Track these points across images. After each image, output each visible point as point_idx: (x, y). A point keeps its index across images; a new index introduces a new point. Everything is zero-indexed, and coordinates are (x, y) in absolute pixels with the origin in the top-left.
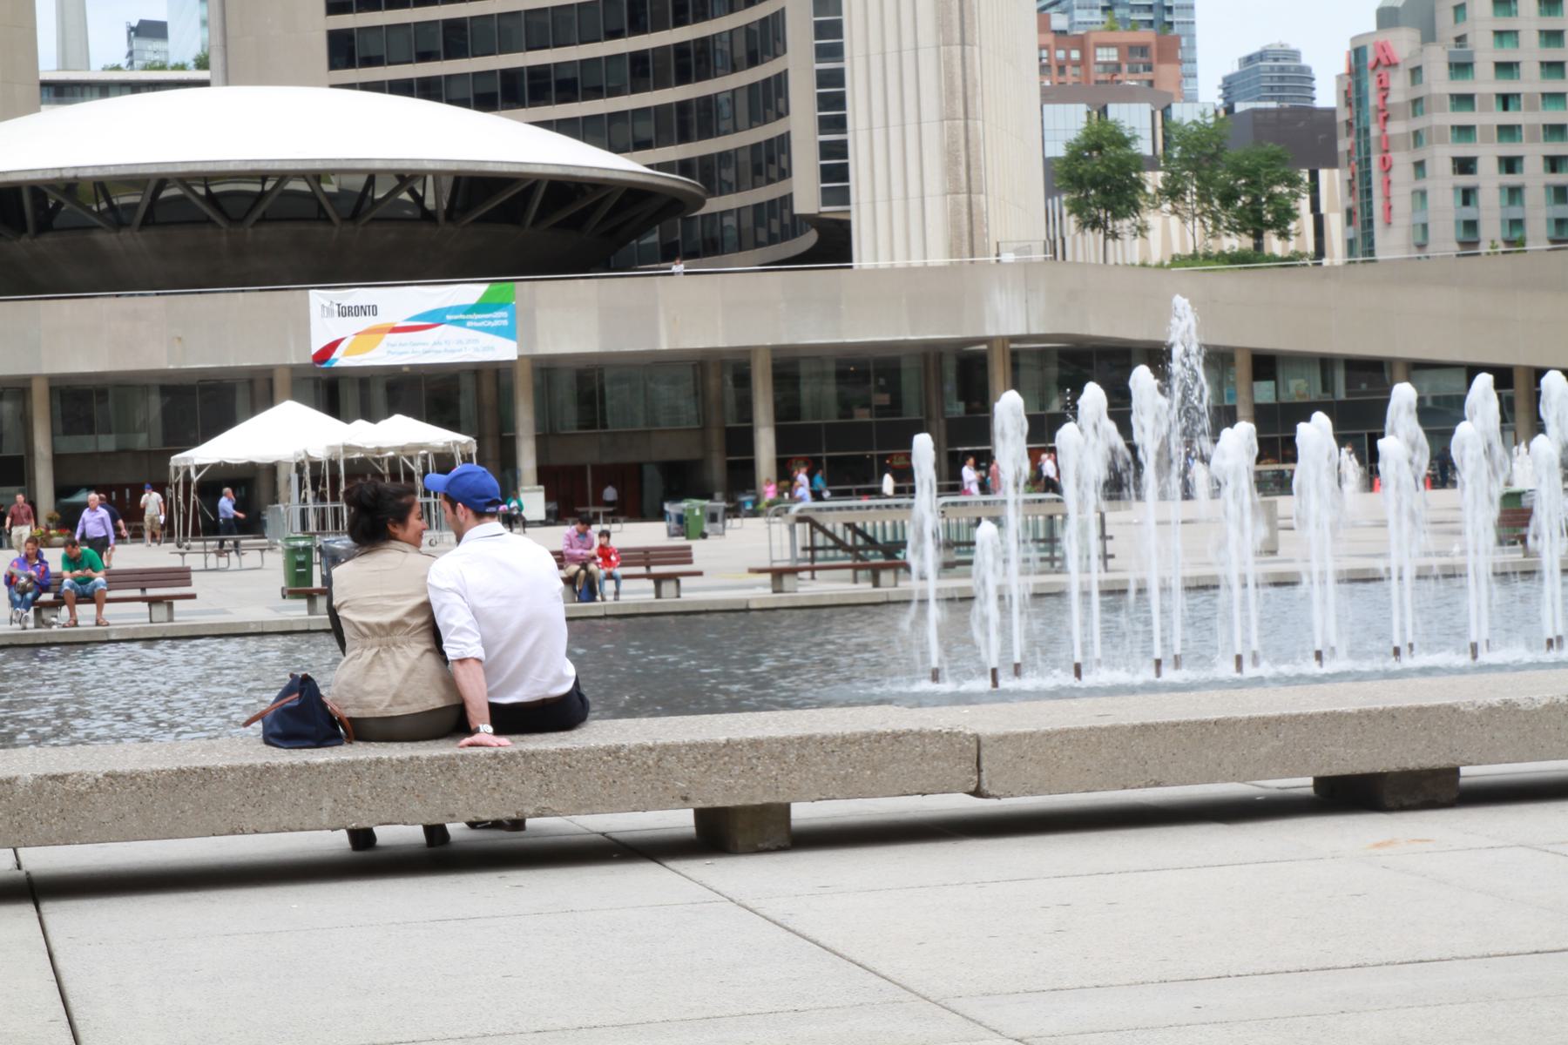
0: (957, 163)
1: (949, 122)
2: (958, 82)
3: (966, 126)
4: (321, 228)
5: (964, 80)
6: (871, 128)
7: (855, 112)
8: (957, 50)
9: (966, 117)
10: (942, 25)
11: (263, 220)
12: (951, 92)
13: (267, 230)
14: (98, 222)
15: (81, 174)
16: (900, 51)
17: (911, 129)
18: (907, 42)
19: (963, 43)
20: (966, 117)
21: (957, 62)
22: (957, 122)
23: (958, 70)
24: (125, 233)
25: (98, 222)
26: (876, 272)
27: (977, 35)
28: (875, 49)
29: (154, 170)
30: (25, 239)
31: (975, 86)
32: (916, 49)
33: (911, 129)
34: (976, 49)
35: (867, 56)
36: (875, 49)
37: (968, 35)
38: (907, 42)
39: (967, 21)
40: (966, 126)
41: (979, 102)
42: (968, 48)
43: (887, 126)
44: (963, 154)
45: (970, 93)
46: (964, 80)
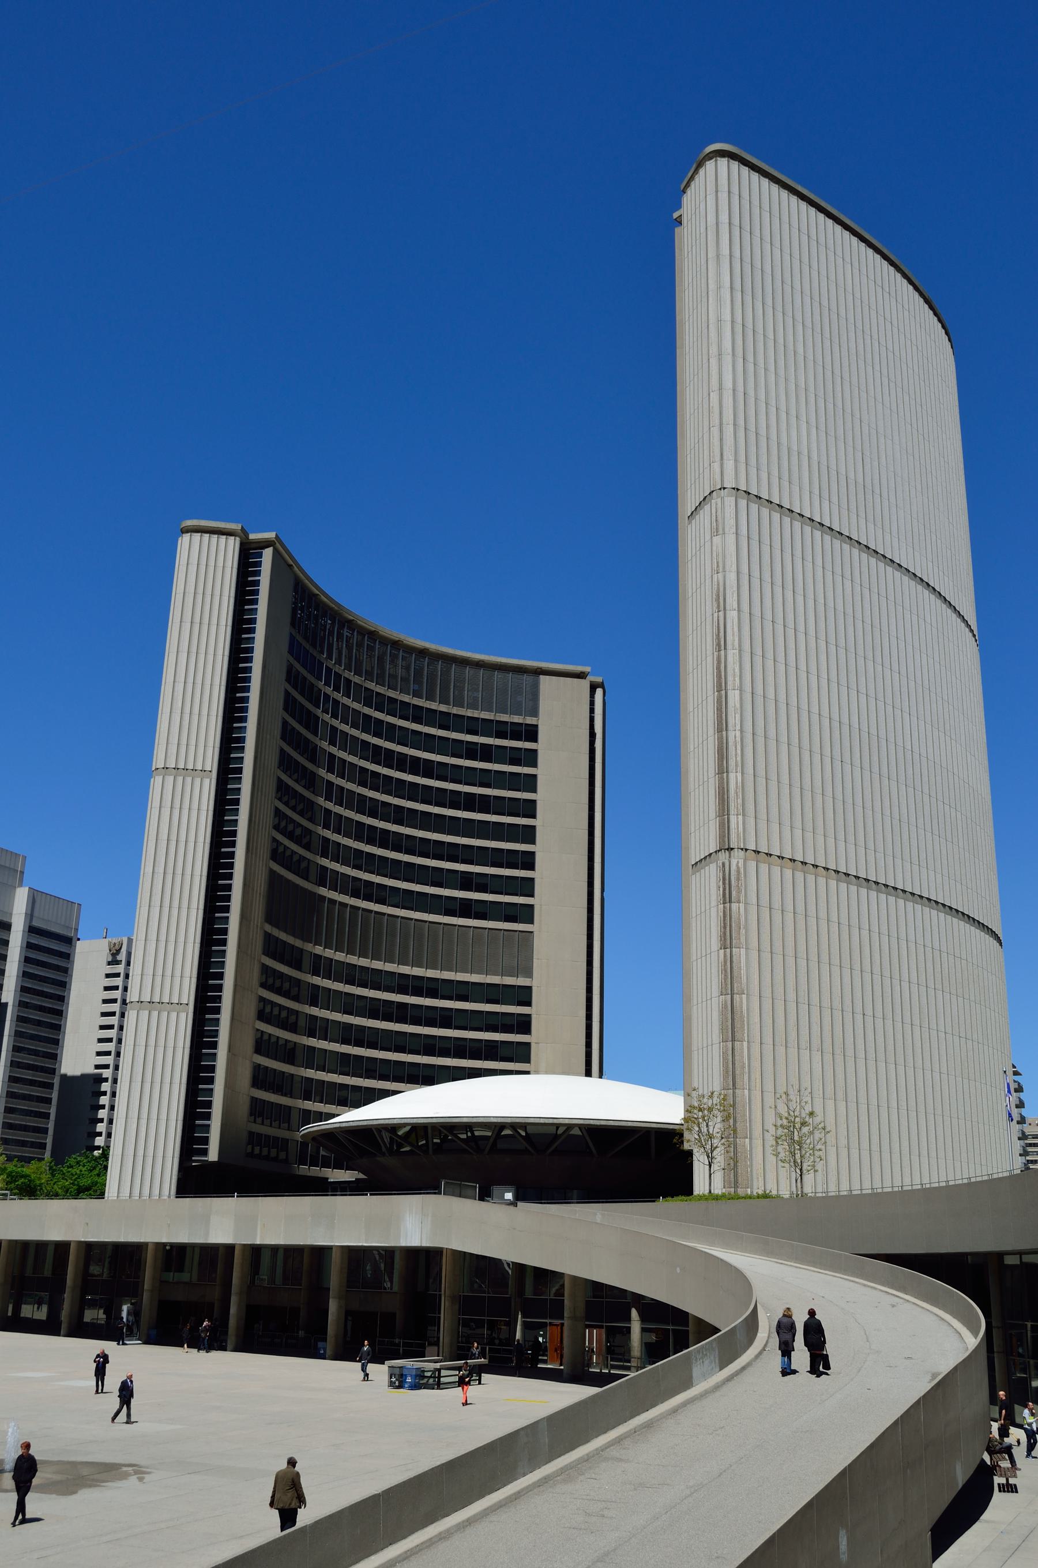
2: (730, 1066)
3: (734, 1093)
5: (733, 1064)
8: (730, 1044)
10: (723, 1030)
12: (727, 1072)
19: (733, 1040)
21: (730, 1052)
27: (746, 1035)
31: (743, 1067)
37: (738, 1035)
39: (737, 1025)
40: (734, 1093)
42: (737, 1044)
45: (737, 1072)
46: (733, 1064)
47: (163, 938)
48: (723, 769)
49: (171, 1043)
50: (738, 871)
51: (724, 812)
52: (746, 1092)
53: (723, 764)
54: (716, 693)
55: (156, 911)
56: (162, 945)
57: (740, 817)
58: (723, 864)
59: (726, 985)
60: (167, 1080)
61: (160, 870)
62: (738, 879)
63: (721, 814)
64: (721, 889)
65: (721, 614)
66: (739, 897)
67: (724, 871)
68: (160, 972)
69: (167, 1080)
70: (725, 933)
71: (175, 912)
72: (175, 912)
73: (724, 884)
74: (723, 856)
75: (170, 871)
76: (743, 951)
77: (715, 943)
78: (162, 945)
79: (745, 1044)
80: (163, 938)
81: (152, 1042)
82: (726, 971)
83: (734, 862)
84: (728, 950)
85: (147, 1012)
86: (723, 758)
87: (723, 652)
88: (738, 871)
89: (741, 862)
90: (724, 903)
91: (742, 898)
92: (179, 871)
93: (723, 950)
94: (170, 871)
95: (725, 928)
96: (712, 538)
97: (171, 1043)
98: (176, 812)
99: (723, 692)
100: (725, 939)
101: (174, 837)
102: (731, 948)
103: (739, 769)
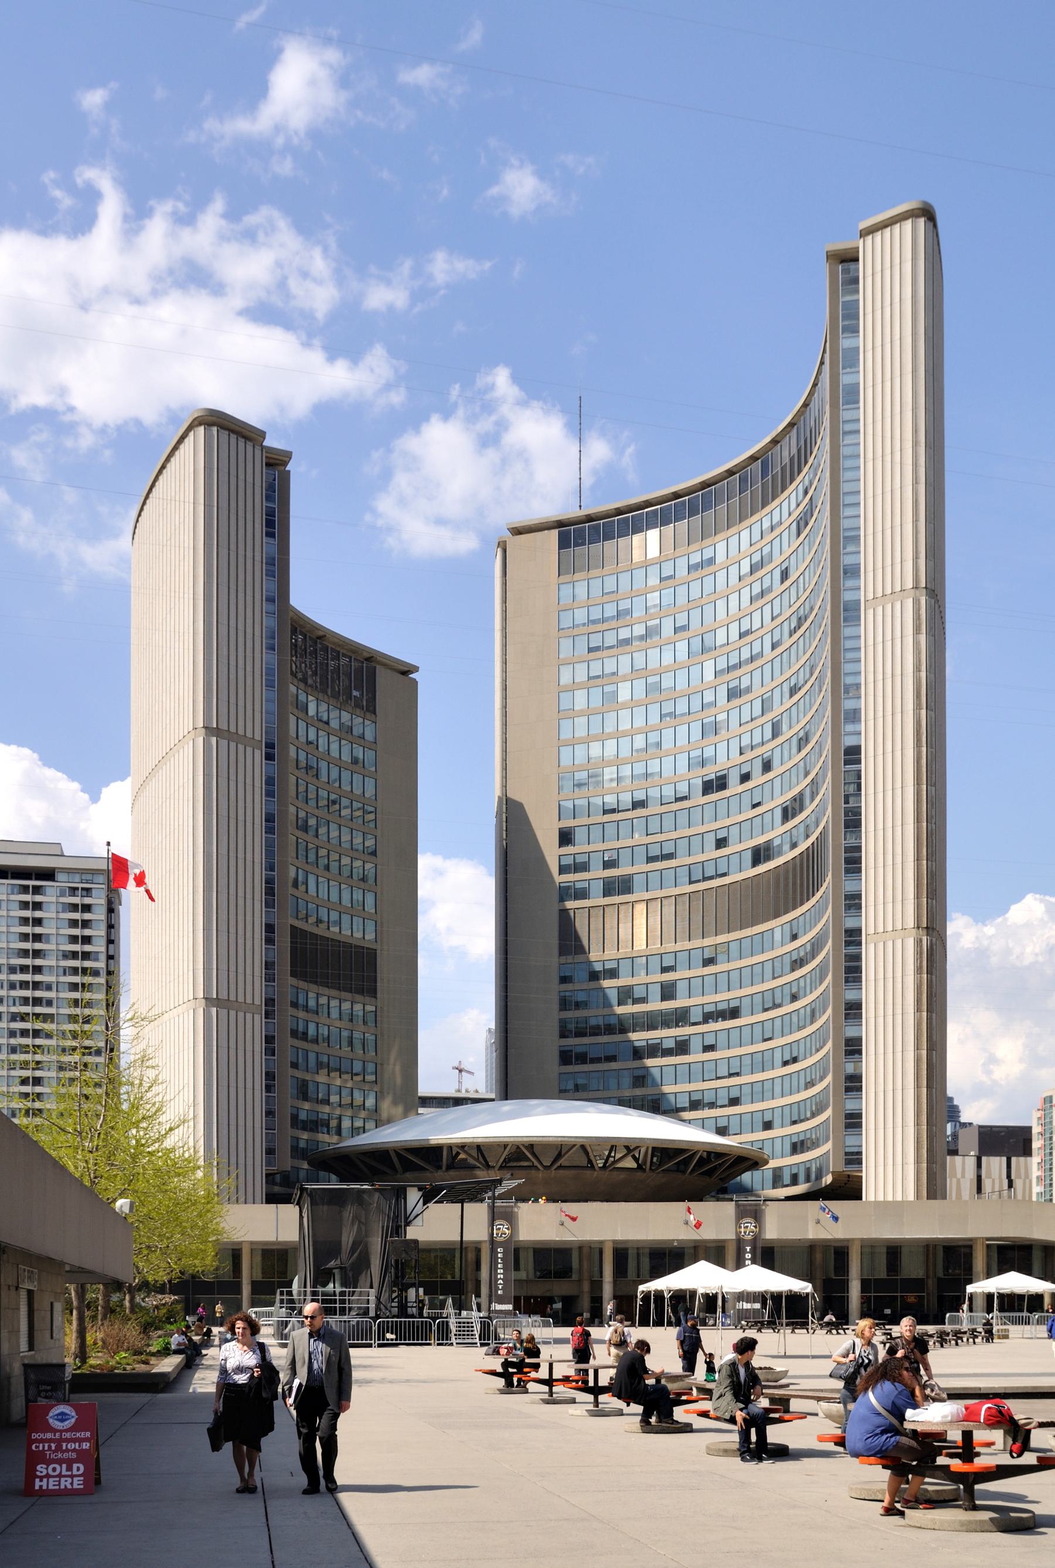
4: (588, 1172)
11: (561, 1167)
13: (561, 1172)
14: (478, 1165)
15: (475, 1140)
24: (491, 1172)
25: (478, 1165)
26: (877, 1204)
29: (512, 1140)
30: (440, 1173)
34: (934, 1090)
53: (922, 852)
58: (921, 940)
62: (932, 954)
67: (921, 946)
84: (925, 1014)
89: (934, 940)
91: (934, 970)
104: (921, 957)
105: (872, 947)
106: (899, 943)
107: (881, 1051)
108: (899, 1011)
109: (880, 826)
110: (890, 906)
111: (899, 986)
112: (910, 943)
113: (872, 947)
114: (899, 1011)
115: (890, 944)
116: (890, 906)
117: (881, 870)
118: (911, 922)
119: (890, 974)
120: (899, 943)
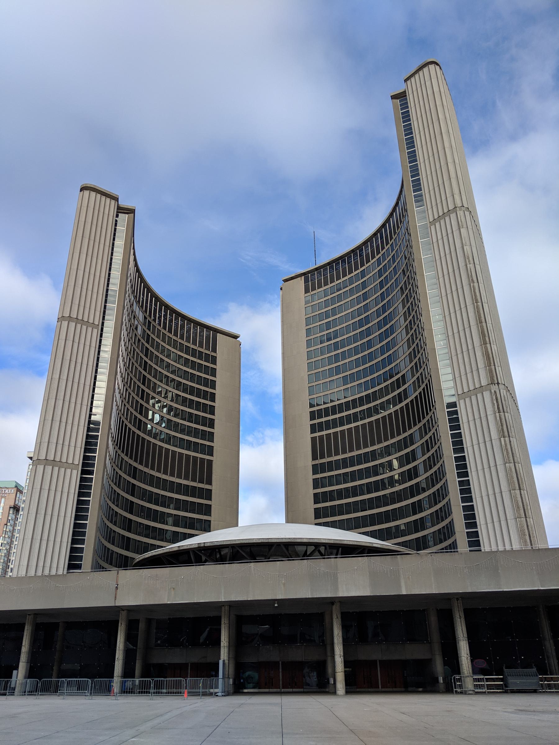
0: (525, 535)
1: (519, 519)
3: (526, 520)
5: (523, 503)
6: (487, 524)
7: (480, 519)
8: (518, 492)
9: (526, 517)
16: (495, 494)
17: (503, 523)
18: (497, 490)
19: (520, 489)
20: (526, 517)
21: (519, 496)
22: (522, 519)
23: (519, 499)
28: (484, 494)
31: (527, 505)
32: (501, 492)
33: (503, 523)
35: (482, 497)
36: (484, 494)
37: (521, 488)
38: (497, 490)
40: (526, 520)
41: (530, 511)
42: (522, 491)
43: (493, 522)
44: (526, 531)
46: (523, 503)
47: (64, 420)
48: (486, 342)
49: (66, 490)
50: (504, 396)
51: (490, 363)
52: (531, 520)
53: (485, 339)
54: (475, 304)
55: (60, 403)
56: (63, 424)
57: (500, 368)
58: (495, 392)
59: (509, 458)
60: (62, 514)
61: (64, 377)
63: (489, 365)
64: (496, 405)
65: (472, 266)
66: (507, 410)
68: (61, 442)
69: (62, 514)
70: (503, 429)
71: (72, 405)
72: (72, 405)
73: (497, 402)
74: (494, 388)
75: (70, 379)
76: (514, 439)
77: (494, 435)
78: (63, 424)
79: (525, 492)
80: (64, 420)
81: (53, 488)
82: (507, 450)
83: (502, 391)
84: (507, 439)
85: (51, 467)
86: (485, 336)
87: (476, 285)
88: (504, 396)
90: (499, 412)
91: (509, 411)
92: (76, 380)
93: (502, 439)
94: (70, 379)
95: (502, 425)
96: (459, 229)
97: (66, 490)
98: (76, 345)
99: (480, 304)
100: (503, 432)
101: (74, 359)
102: (509, 437)
103: (495, 343)
104: (497, 402)
105: (462, 402)
106: (479, 396)
107: (480, 467)
108: (487, 439)
109: (455, 331)
110: (469, 375)
111: (484, 423)
112: (487, 394)
113: (462, 402)
114: (487, 439)
115: (473, 398)
116: (469, 375)
117: (460, 356)
118: (484, 382)
119: (477, 416)
120: (479, 396)
